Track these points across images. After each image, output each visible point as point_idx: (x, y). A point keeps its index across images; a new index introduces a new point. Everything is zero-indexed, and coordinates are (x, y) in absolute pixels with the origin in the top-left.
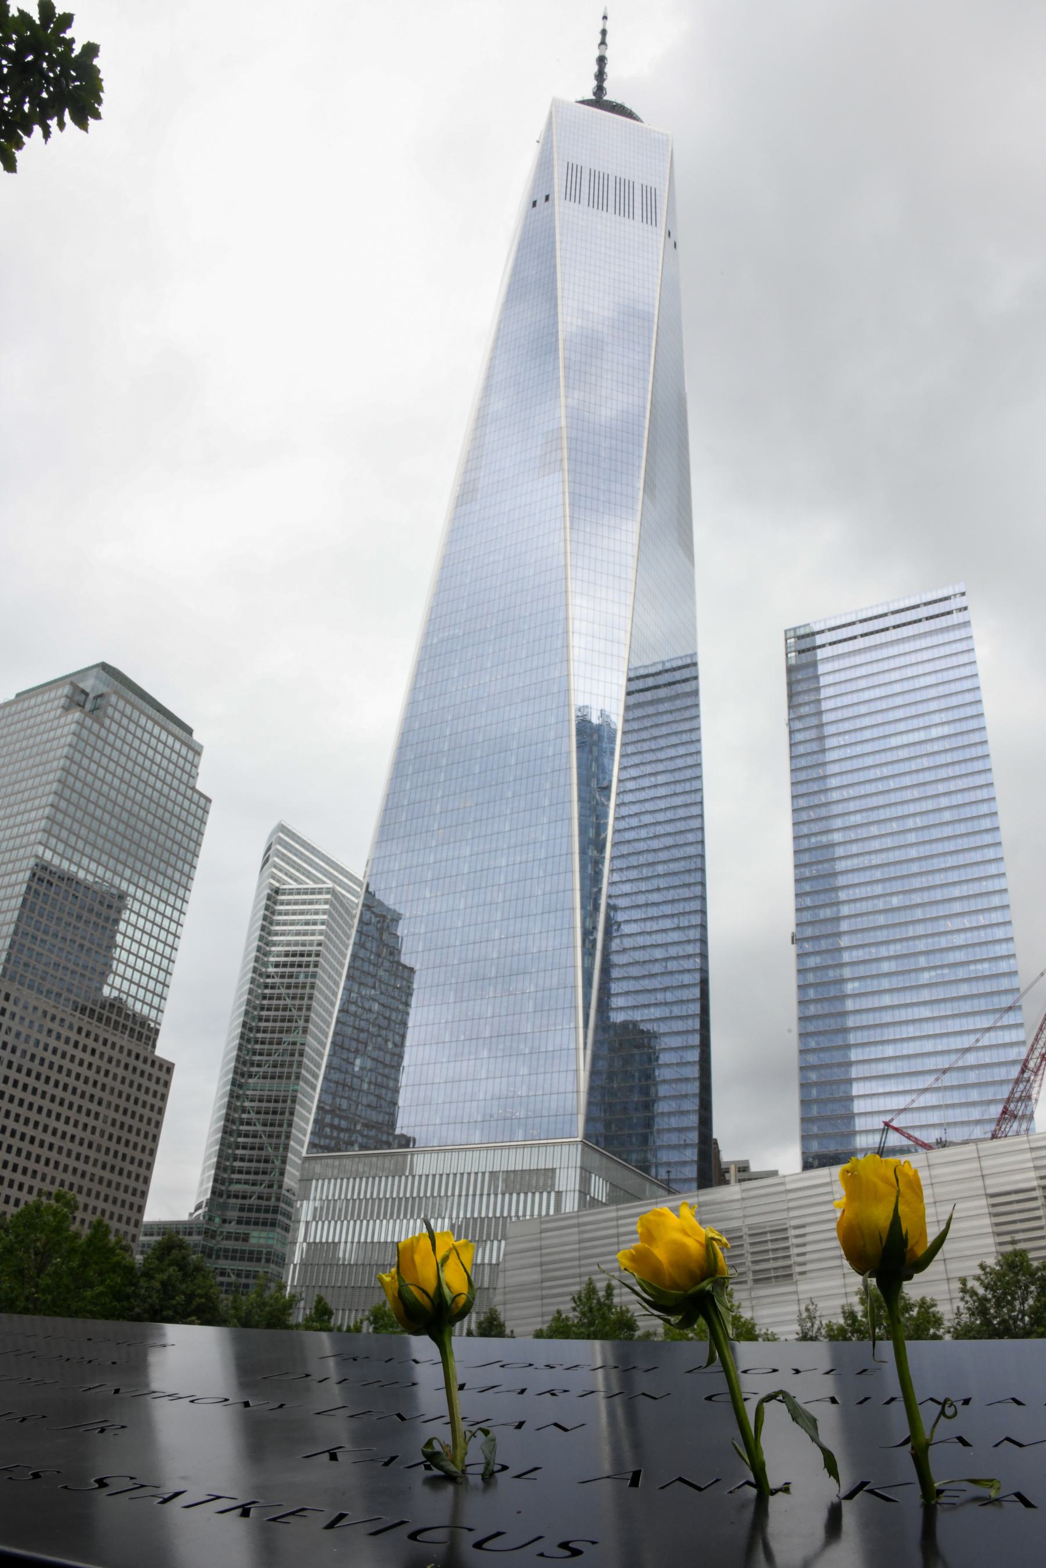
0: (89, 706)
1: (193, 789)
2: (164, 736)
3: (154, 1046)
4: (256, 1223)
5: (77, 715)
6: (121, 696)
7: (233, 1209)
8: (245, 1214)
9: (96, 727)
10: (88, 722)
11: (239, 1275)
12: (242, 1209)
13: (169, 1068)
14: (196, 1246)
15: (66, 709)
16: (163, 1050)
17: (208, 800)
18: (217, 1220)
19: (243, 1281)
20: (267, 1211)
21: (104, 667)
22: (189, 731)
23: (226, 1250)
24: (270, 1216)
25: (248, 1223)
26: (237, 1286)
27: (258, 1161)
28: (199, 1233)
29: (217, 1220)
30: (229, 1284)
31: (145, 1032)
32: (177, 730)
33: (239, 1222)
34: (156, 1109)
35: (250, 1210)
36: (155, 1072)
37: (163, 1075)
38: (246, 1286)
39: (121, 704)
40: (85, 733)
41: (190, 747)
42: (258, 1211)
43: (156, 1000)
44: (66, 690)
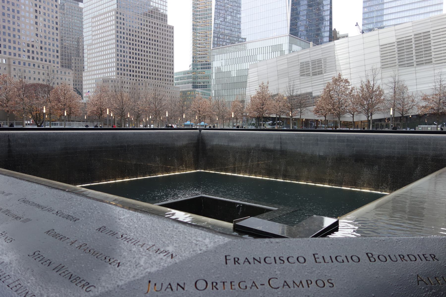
3: (167, 22)
4: (206, 68)
7: (199, 65)
8: (203, 66)
11: (204, 83)
12: (202, 65)
13: (173, 28)
16: (169, 23)
18: (196, 69)
19: (205, 84)
20: (208, 65)
24: (209, 66)
25: (204, 68)
26: (204, 85)
28: (191, 73)
29: (196, 69)
30: (202, 86)
31: (164, 17)
33: (202, 69)
35: (204, 65)
36: (169, 29)
37: (171, 30)
38: (206, 85)
42: (206, 65)
43: (164, 7)
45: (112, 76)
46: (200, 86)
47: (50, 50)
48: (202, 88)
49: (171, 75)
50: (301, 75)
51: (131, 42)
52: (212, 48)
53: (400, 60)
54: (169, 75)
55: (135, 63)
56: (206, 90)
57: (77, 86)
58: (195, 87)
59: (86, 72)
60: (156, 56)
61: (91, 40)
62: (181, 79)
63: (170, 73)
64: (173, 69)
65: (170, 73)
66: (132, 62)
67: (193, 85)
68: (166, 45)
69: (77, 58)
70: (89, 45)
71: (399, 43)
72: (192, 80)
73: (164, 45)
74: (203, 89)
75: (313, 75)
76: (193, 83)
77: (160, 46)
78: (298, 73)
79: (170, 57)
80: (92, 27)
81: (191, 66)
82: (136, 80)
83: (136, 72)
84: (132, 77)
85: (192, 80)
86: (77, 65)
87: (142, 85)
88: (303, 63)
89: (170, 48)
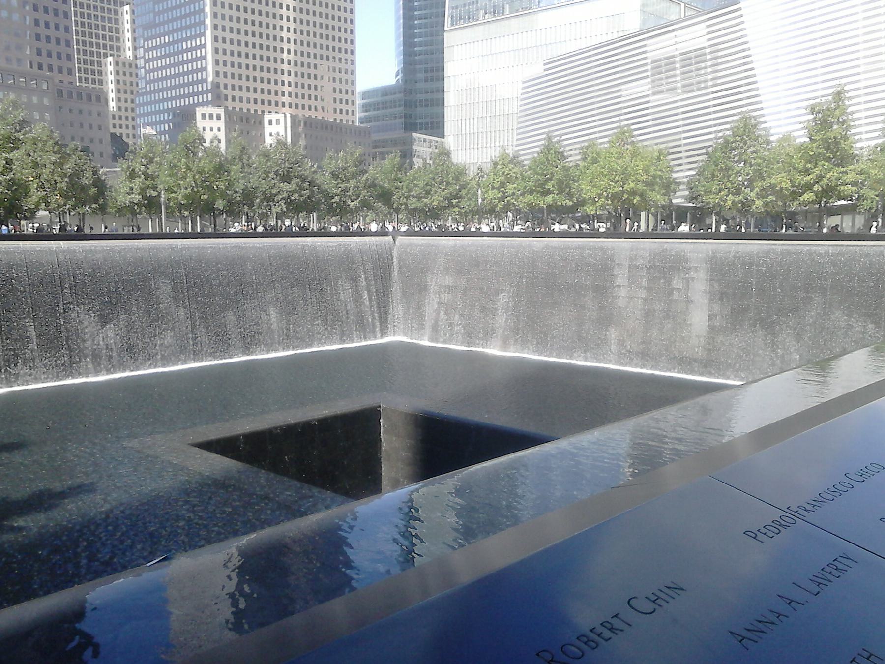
14: (400, 101)
23: (421, 101)
27: (426, 36)
28: (400, 93)
33: (426, 81)
34: (348, 10)
46: (421, 124)
47: (48, 39)
48: (426, 129)
49: (349, 97)
51: (249, 17)
52: (446, 28)
54: (344, 97)
55: (258, 69)
57: (124, 131)
59: (143, 94)
60: (312, 50)
61: (152, 15)
63: (347, 93)
64: (353, 83)
65: (347, 93)
66: (251, 68)
67: (405, 123)
68: (336, 23)
72: (402, 108)
73: (331, 23)
74: (424, 131)
76: (405, 117)
77: (321, 24)
79: (346, 52)
82: (263, 112)
83: (262, 91)
85: (402, 108)
86: (121, 78)
88: (660, 60)
89: (346, 31)
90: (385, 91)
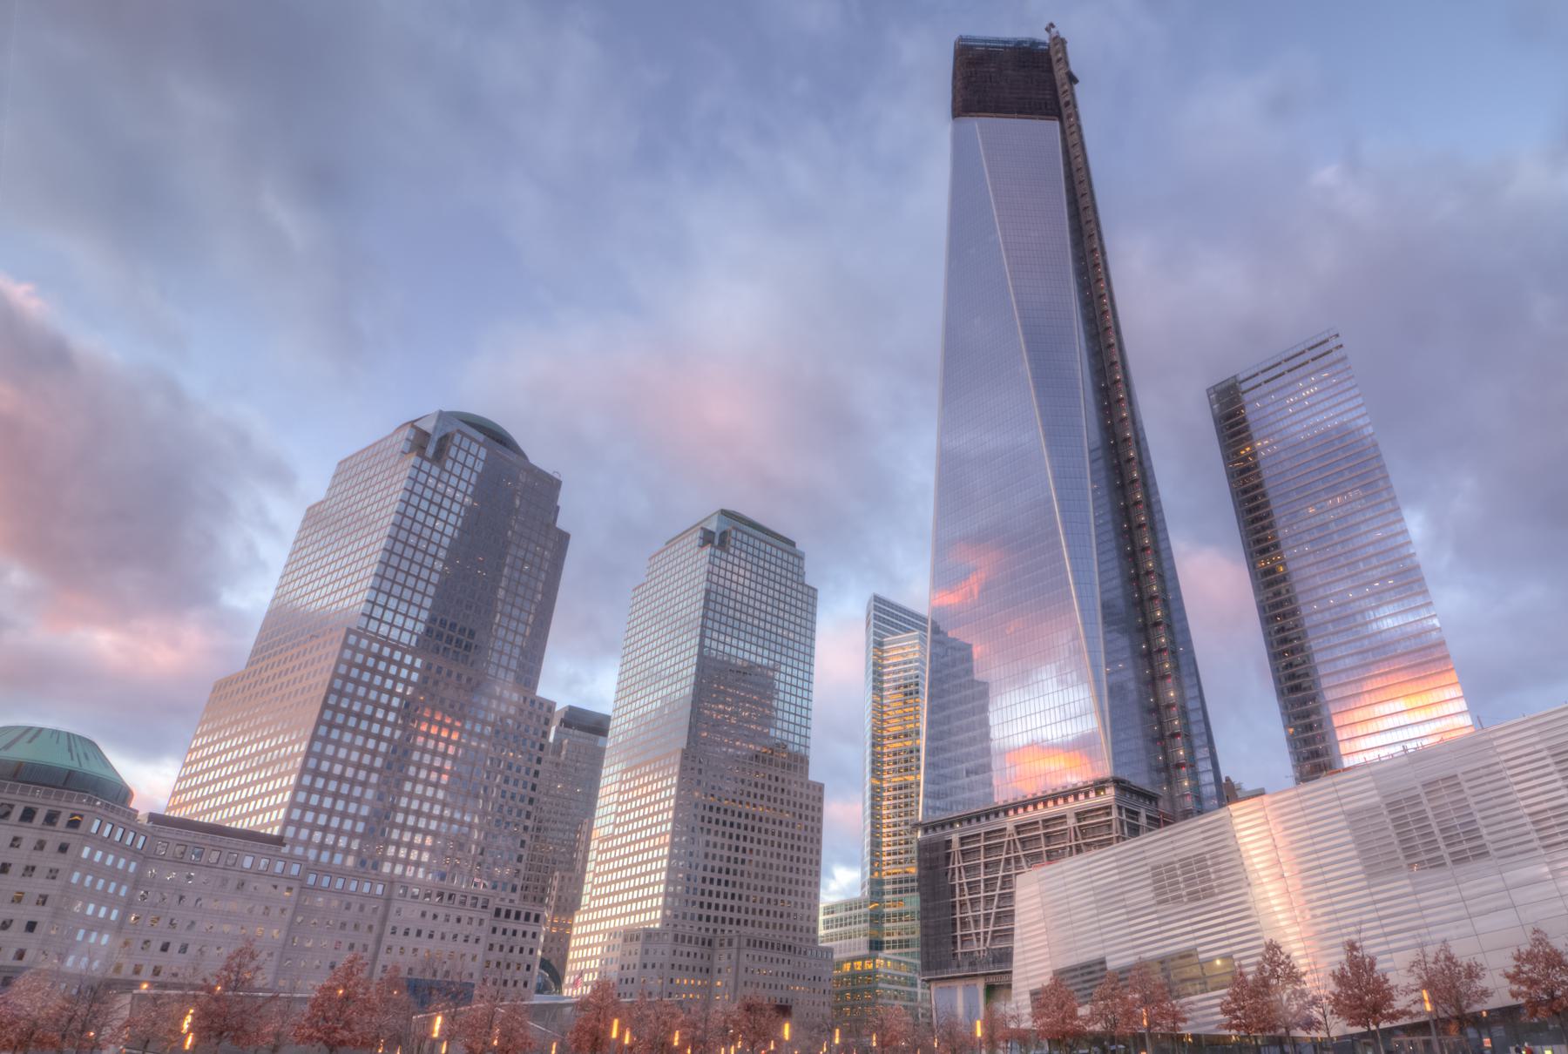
0: (716, 542)
1: (803, 584)
2: (774, 551)
5: (708, 550)
6: (737, 529)
9: (724, 555)
10: (718, 553)
15: (702, 546)
17: (815, 590)
21: (724, 513)
22: (793, 544)
32: (787, 547)
39: (739, 535)
40: (717, 561)
41: (795, 555)
44: (699, 534)
45: (651, 922)
50: (1160, 903)
53: (1410, 852)
56: (907, 954)
58: (876, 945)
62: (840, 922)
69: (567, 875)
70: (603, 840)
71: (1394, 807)
75: (1191, 901)
78: (1146, 895)
80: (620, 793)
81: (867, 887)
84: (703, 924)
87: (730, 943)
90: (849, 905)
